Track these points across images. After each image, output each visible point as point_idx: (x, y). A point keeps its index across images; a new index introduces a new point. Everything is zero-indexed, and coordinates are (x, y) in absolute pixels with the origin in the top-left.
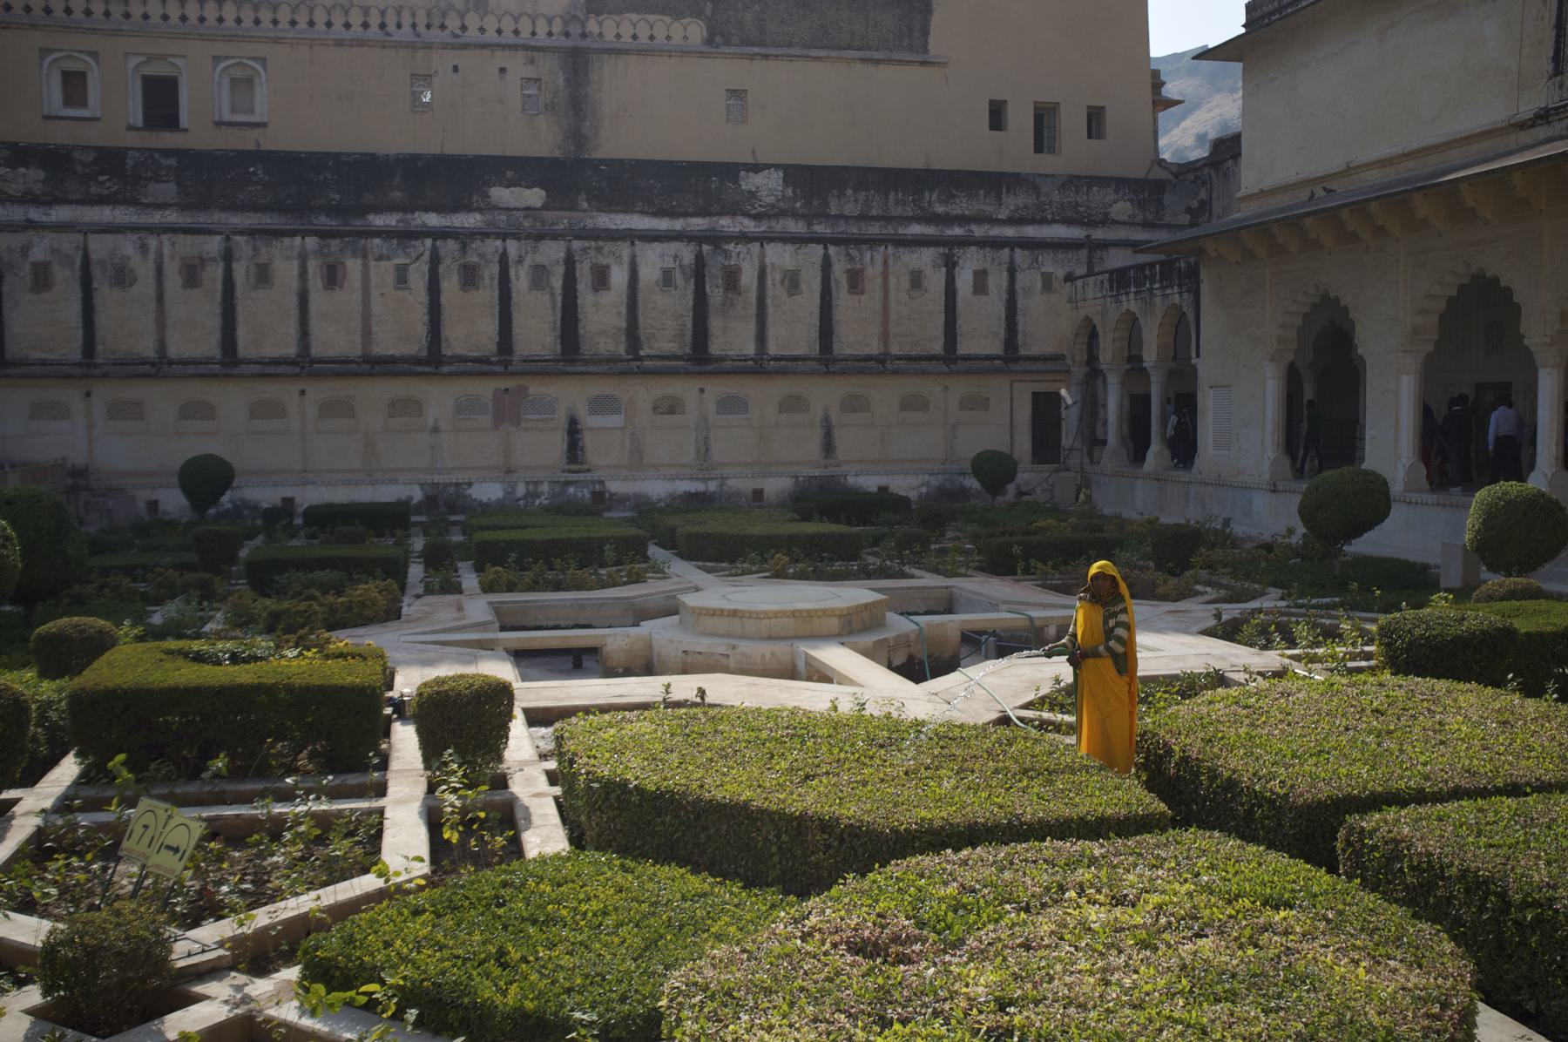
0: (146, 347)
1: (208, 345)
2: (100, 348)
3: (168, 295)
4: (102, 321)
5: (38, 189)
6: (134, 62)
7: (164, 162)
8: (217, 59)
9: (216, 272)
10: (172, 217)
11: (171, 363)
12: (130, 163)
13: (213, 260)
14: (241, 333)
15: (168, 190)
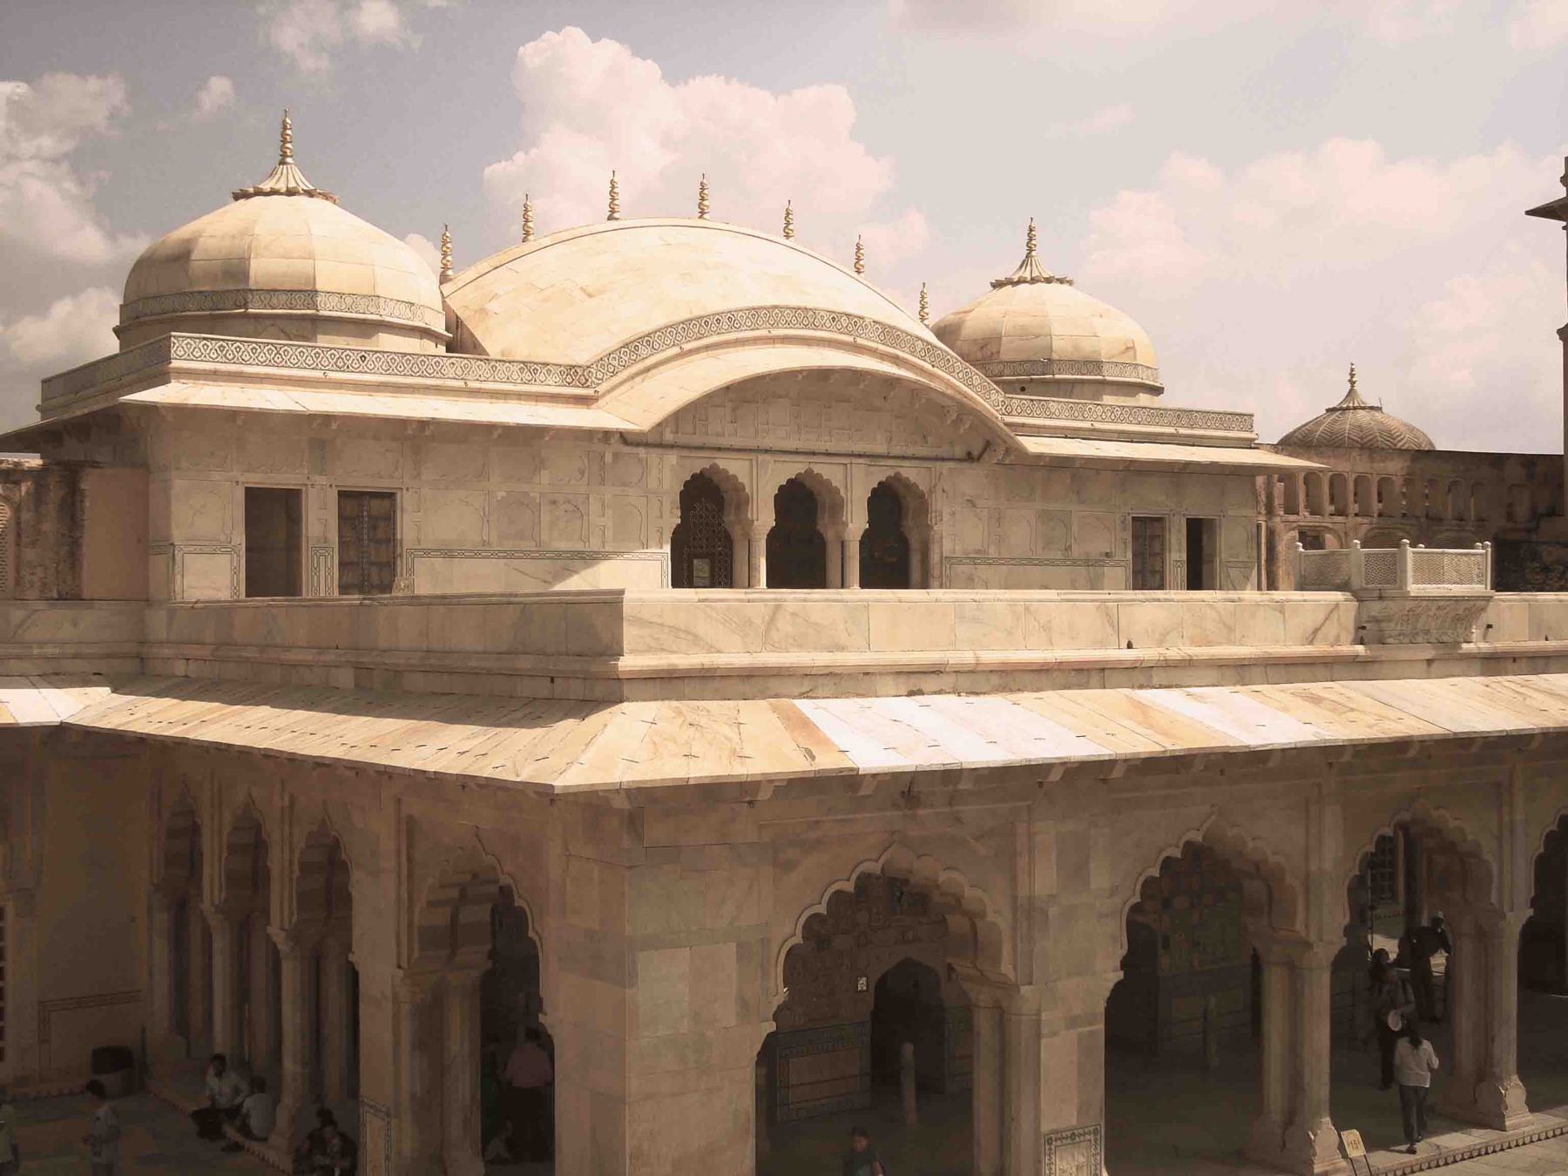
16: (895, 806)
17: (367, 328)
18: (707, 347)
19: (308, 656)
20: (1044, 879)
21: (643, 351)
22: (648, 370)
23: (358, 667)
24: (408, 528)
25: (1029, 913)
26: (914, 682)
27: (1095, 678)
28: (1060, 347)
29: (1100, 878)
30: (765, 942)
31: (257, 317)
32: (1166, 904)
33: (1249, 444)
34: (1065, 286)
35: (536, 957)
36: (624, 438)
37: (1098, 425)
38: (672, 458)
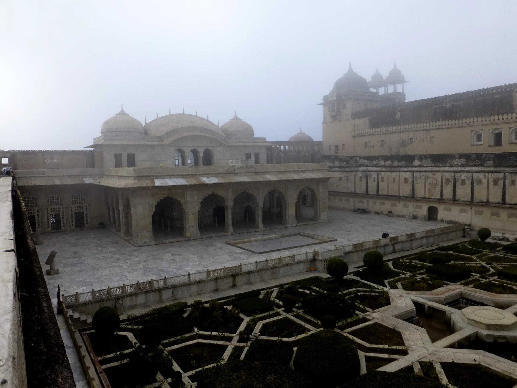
0: (484, 199)
1: (499, 200)
2: (474, 198)
3: (490, 187)
4: (475, 192)
5: (464, 163)
6: (491, 130)
7: (491, 156)
8: (510, 128)
9: (501, 182)
10: (492, 169)
11: (490, 203)
12: (483, 157)
13: (501, 179)
14: (507, 197)
15: (491, 163)
19: (114, 174)
20: (188, 198)
23: (118, 176)
24: (136, 158)
29: (196, 198)
36: (166, 145)
38: (174, 148)
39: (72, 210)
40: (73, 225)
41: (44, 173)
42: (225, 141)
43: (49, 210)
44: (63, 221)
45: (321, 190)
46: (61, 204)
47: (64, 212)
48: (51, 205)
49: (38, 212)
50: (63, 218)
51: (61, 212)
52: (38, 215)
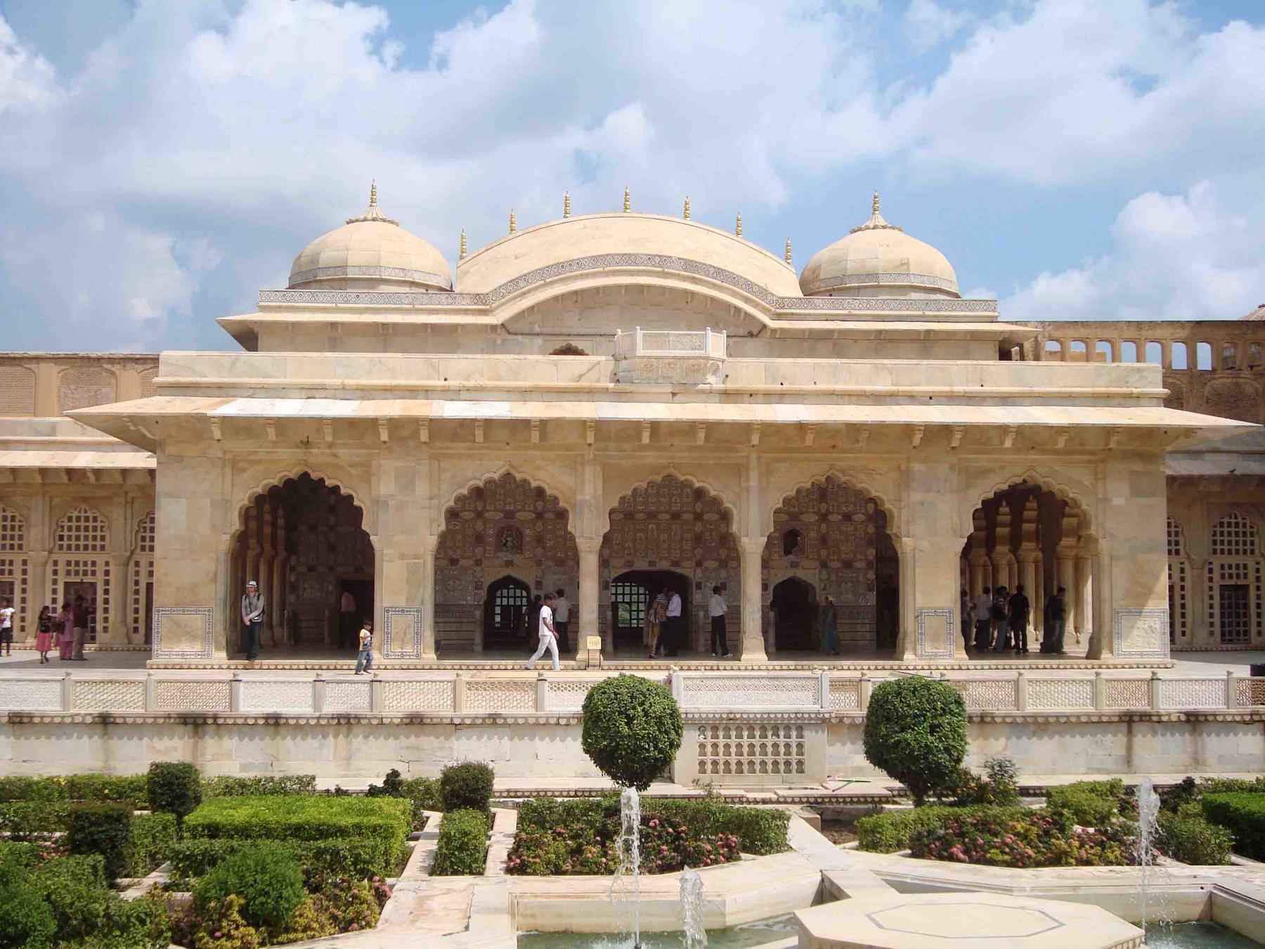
16: (297, 447)
17: (373, 282)
18: (562, 280)
20: (385, 487)
21: (522, 284)
22: (524, 294)
25: (376, 501)
26: (310, 393)
27: (422, 394)
28: (851, 267)
29: (422, 489)
30: (227, 502)
31: (321, 281)
32: (699, 564)
33: (992, 320)
34: (896, 232)
35: (373, 582)
37: (854, 312)
38: (539, 340)
39: (137, 573)
40: (136, 630)
41: (53, 429)
42: (779, 317)
43: (62, 568)
44: (106, 610)
45: (1118, 501)
46: (103, 548)
47: (112, 577)
48: (69, 547)
49: (25, 572)
50: (106, 601)
51: (99, 579)
52: (24, 581)
